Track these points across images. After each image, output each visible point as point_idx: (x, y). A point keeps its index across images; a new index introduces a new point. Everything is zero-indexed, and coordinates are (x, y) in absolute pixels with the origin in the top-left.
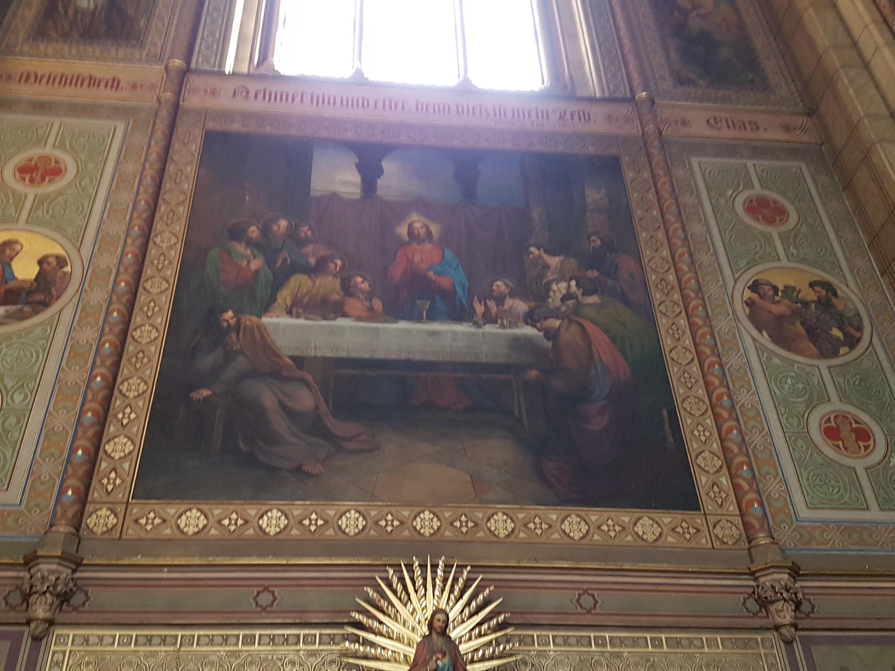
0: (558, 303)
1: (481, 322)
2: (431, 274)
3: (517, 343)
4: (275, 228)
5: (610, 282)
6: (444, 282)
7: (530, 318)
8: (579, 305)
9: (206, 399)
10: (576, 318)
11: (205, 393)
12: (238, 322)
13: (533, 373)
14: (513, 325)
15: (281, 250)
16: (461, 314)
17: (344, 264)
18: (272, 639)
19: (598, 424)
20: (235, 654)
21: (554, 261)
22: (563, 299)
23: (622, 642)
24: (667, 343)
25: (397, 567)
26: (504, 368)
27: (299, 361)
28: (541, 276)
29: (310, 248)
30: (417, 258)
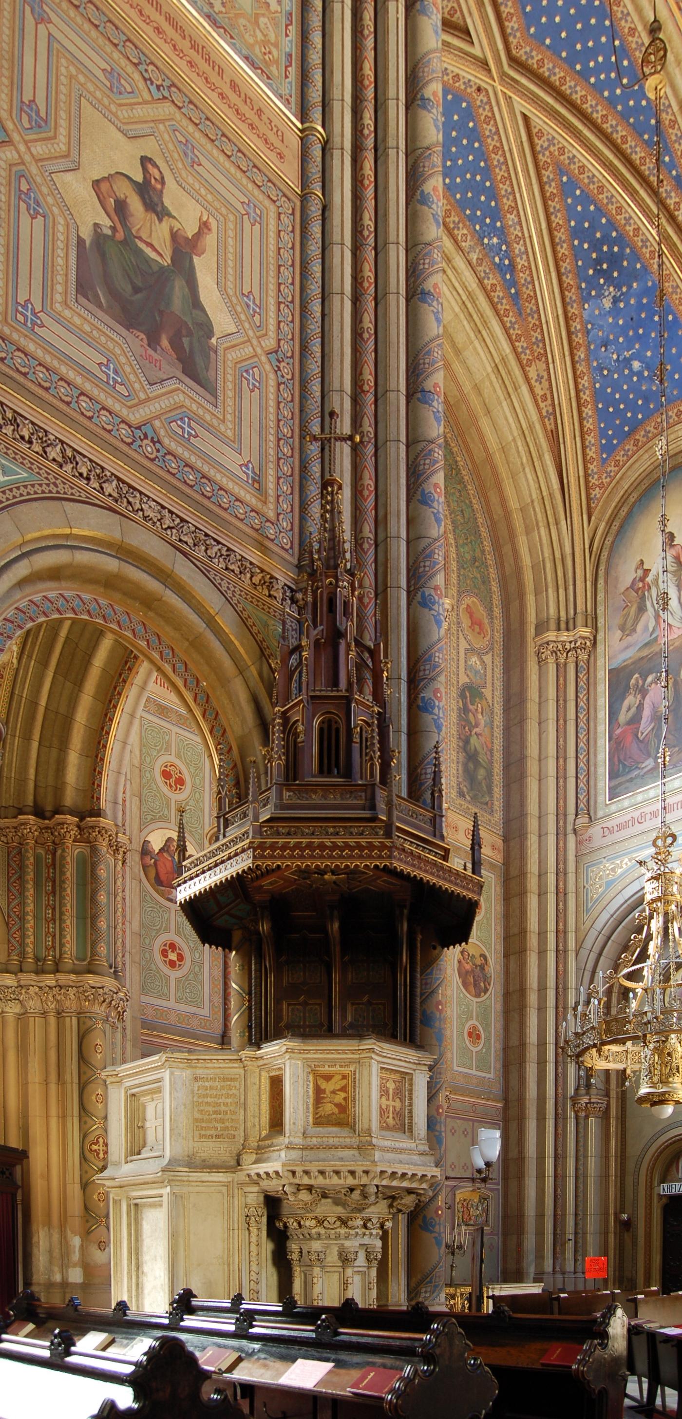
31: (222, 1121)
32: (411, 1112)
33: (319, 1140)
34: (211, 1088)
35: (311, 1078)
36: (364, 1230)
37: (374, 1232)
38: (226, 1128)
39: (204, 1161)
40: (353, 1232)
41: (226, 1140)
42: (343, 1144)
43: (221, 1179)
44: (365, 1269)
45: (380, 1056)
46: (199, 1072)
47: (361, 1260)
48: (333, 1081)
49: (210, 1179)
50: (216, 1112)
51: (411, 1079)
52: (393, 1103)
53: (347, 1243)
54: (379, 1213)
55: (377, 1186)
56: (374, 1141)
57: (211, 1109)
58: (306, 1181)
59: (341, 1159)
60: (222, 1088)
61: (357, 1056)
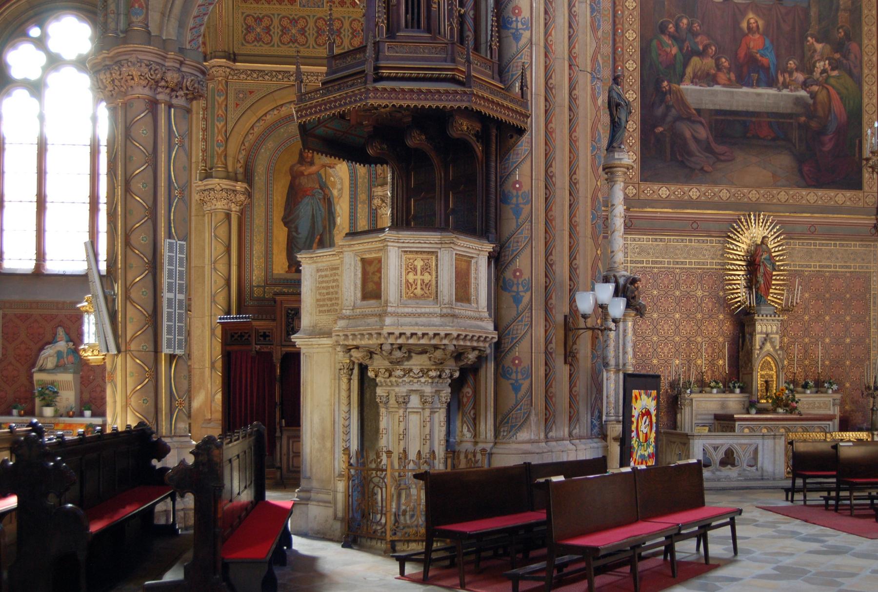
0: (818, 75)
1: (781, 88)
2: (758, 55)
3: (798, 101)
4: (681, 25)
5: (845, 61)
6: (764, 61)
7: (805, 85)
8: (828, 77)
9: (661, 132)
10: (826, 86)
11: (661, 129)
12: (670, 88)
13: (803, 119)
14: (796, 89)
15: (686, 40)
16: (771, 83)
17: (716, 49)
18: (699, 241)
19: (828, 147)
20: (686, 246)
21: (819, 47)
22: (821, 73)
23: (823, 245)
24: (866, 100)
25: (744, 215)
26: (789, 116)
27: (699, 111)
28: (812, 57)
29: (699, 38)
30: (752, 45)
31: (330, 299)
32: (437, 283)
33: (361, 310)
34: (326, 276)
35: (359, 264)
37: (423, 380)
38: (332, 305)
39: (320, 329)
40: (400, 380)
44: (420, 410)
46: (320, 265)
47: (415, 401)
49: (323, 342)
50: (328, 294)
51: (437, 257)
52: (422, 277)
53: (397, 389)
54: (421, 365)
55: (392, 344)
56: (389, 309)
57: (325, 291)
58: (350, 342)
59: (368, 325)
60: (331, 275)
61: (382, 245)
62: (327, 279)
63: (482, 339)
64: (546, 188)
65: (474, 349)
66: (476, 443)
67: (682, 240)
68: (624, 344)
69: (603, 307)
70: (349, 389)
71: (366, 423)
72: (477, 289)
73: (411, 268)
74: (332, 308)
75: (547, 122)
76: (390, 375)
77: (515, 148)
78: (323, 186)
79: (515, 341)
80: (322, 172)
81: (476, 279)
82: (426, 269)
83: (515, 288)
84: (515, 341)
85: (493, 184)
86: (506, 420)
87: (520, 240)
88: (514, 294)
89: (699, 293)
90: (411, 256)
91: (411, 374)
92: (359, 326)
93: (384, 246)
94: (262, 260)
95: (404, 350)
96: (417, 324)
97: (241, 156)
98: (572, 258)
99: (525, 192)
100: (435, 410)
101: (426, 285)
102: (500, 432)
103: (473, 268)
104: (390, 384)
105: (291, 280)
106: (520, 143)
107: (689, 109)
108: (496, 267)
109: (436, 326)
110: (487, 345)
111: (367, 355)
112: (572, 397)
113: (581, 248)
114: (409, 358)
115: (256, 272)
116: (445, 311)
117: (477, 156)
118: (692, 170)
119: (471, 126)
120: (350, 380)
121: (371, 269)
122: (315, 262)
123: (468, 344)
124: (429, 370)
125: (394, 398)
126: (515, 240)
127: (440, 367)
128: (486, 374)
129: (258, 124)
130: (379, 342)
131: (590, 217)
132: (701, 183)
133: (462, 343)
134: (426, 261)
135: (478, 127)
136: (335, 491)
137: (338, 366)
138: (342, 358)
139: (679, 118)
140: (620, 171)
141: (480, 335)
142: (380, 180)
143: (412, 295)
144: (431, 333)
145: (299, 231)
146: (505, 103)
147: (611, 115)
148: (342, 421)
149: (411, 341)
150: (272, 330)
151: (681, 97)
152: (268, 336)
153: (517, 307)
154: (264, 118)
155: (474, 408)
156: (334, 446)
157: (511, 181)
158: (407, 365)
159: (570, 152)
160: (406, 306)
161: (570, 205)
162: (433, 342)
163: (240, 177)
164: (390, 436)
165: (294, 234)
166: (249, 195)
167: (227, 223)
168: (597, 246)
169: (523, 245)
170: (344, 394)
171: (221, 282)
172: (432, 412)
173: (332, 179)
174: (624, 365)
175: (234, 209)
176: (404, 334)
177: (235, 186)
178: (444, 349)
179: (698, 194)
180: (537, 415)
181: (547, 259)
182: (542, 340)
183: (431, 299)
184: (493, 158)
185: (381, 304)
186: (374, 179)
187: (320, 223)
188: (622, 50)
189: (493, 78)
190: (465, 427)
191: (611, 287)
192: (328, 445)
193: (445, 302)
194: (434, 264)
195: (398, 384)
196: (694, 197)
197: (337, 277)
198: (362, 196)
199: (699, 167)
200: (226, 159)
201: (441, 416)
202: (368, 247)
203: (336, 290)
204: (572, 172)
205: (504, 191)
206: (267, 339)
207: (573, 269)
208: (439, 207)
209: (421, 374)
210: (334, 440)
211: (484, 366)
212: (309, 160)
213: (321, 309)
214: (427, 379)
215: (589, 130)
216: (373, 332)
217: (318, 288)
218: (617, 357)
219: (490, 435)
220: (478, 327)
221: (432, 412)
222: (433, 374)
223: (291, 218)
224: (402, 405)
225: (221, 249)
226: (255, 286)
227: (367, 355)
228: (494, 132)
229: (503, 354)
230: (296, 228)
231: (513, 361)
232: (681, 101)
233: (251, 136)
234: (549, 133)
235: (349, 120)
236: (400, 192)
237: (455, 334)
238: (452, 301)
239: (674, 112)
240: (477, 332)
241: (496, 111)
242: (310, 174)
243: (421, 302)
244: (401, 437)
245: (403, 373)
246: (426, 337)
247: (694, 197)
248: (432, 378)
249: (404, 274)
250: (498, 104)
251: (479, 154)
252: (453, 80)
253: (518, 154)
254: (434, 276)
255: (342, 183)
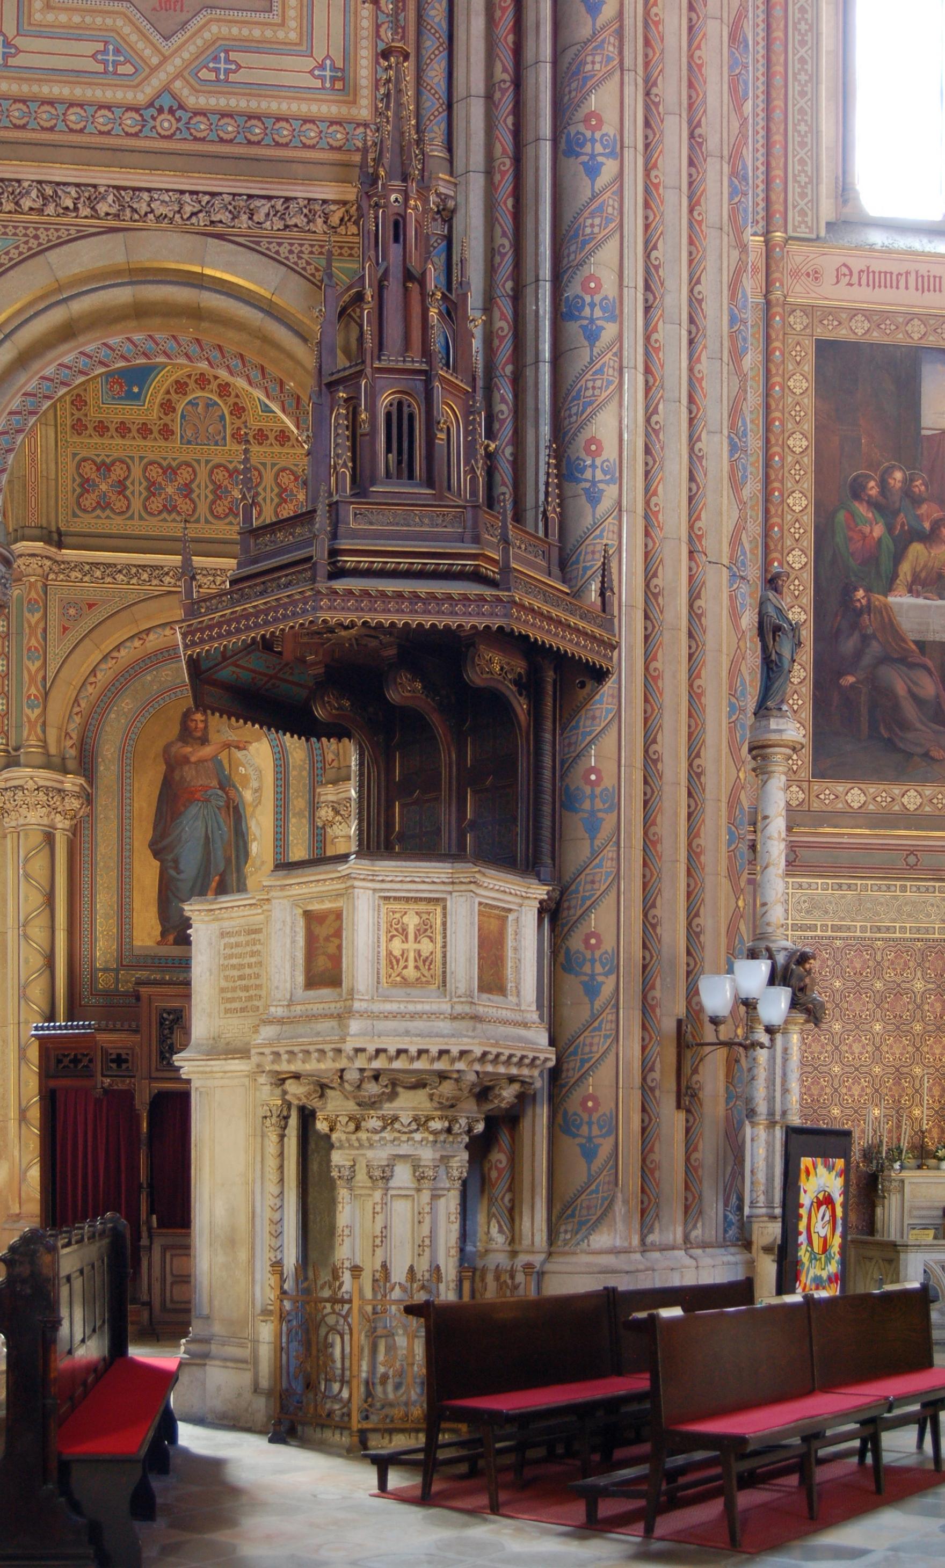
9: (852, 686)
11: (851, 679)
12: (869, 600)
27: (921, 645)
31: (246, 988)
32: (444, 956)
34: (237, 945)
35: (301, 923)
36: (397, 1135)
37: (418, 1136)
38: (250, 998)
39: (228, 1044)
40: (376, 1137)
41: (251, 1013)
42: (328, 1012)
43: (243, 1067)
45: (372, 880)
46: (226, 924)
47: (403, 1176)
48: (328, 922)
50: (241, 978)
51: (445, 908)
52: (417, 946)
53: (370, 1154)
54: (414, 1109)
55: (362, 1070)
56: (357, 1005)
57: (236, 973)
58: (284, 1067)
60: (247, 944)
61: (343, 886)
62: (239, 950)
63: (527, 1061)
64: (646, 782)
65: (512, 1079)
66: (514, 1254)
67: (888, 887)
68: (784, 1075)
69: (749, 1005)
70: (281, 1154)
71: (311, 1217)
72: (517, 969)
73: (396, 930)
74: (249, 1004)
75: (649, 658)
76: (358, 1128)
77: (588, 707)
78: (226, 784)
79: (587, 1066)
80: (223, 756)
81: (516, 949)
82: (424, 930)
83: (587, 969)
84: (587, 1066)
85: (547, 773)
86: (569, 1212)
87: (597, 879)
88: (586, 978)
89: (919, 986)
90: (396, 906)
91: (397, 1126)
92: (301, 1036)
93: (347, 888)
94: (113, 921)
95: (384, 1080)
96: (407, 1033)
97: (72, 726)
98: (692, 914)
99: (606, 789)
100: (441, 1192)
101: (424, 961)
102: (558, 1233)
103: (510, 930)
104: (356, 1144)
105: (167, 958)
106: (597, 697)
107: (904, 641)
108: (552, 930)
109: (443, 1036)
110: (536, 1073)
111: (315, 1091)
112: (690, 1169)
113: (708, 896)
114: (393, 1096)
115: (101, 944)
116: (459, 1009)
117: (519, 723)
118: (909, 755)
119: (508, 664)
120: (282, 1137)
121: (322, 931)
122: (218, 920)
123: (502, 1070)
124: (429, 1119)
125: (364, 1171)
126: (589, 878)
127: (450, 1113)
128: (534, 1126)
129: (103, 666)
130: (339, 1066)
131: (725, 837)
132: (924, 780)
133: (489, 1068)
134: (425, 916)
135: (520, 666)
136: (256, 1342)
137: (262, 1112)
138: (269, 1096)
139: (885, 659)
140: (778, 754)
141: (524, 1053)
142: (331, 774)
143: (398, 979)
144: (434, 1050)
145: (182, 867)
146: (573, 621)
147: (765, 648)
148: (268, 1213)
149: (397, 1065)
150: (132, 1049)
151: (890, 619)
152: (126, 1061)
153: (592, 1004)
154: (115, 654)
155: (510, 1189)
156: (253, 1256)
157: (581, 768)
158: (389, 1109)
159: (690, 715)
160: (387, 999)
161: (690, 815)
162: (439, 1066)
163: (71, 764)
164: (358, 1241)
165: (172, 872)
166: (89, 799)
167: (47, 851)
168: (737, 891)
169: (603, 888)
170: (272, 1163)
171: (38, 961)
172: (435, 1197)
173: (242, 770)
174: (784, 1113)
175: (60, 826)
176: (385, 1051)
177: (62, 782)
178: (457, 1080)
179: (919, 801)
180: (626, 1202)
181: (645, 915)
182: (637, 1065)
183: (434, 987)
184: (548, 725)
185: (340, 995)
186: (320, 772)
187: (220, 853)
188: (781, 529)
189: (550, 575)
190: (494, 1223)
191: (763, 968)
192: (243, 1255)
193: (460, 992)
194: (439, 921)
195: (371, 1145)
196: (912, 807)
197: (258, 947)
198: (299, 803)
199: (919, 750)
200: (44, 732)
201: (450, 1203)
202: (318, 889)
203: (256, 970)
204: (694, 753)
205: (567, 786)
206: (124, 1066)
207: (693, 934)
208: (446, 816)
209: (414, 1126)
210: (253, 1248)
211: (529, 1112)
212: (199, 734)
213: (228, 1006)
214: (426, 1135)
215: (724, 674)
216: (327, 1047)
217: (224, 968)
218: (771, 1099)
219: (541, 1238)
220: (521, 1039)
221: (435, 1197)
222: (436, 1125)
223: (165, 842)
224: (380, 1184)
225: (37, 899)
226: (100, 970)
227: (315, 1091)
228: (550, 676)
229: (564, 1090)
230: (176, 861)
231: (584, 1103)
232: (889, 626)
233: (90, 689)
234: (651, 680)
235: (280, 653)
236: (374, 791)
237: (478, 1052)
238: (472, 991)
239: (875, 648)
240: (518, 1048)
241: (556, 635)
242: (201, 761)
243: (414, 992)
244: (378, 1241)
245: (380, 1123)
246: (424, 1056)
247: (912, 807)
248: (435, 1133)
249: (383, 939)
250: (558, 622)
251: (523, 718)
252: (476, 577)
253: (594, 718)
254: (439, 945)
255: (260, 778)
